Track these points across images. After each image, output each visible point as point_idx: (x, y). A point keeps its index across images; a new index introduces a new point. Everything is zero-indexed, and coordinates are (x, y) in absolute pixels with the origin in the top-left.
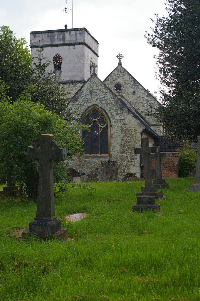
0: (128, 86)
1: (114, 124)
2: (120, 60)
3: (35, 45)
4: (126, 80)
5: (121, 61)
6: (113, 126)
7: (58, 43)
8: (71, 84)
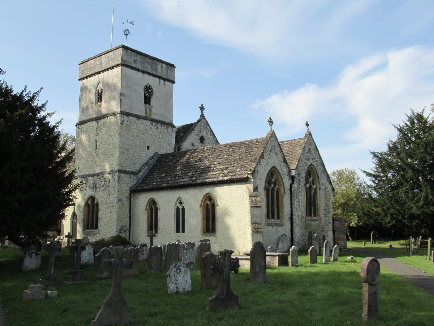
0: (209, 141)
1: (321, 187)
2: (202, 112)
3: (127, 63)
4: (207, 135)
5: (204, 113)
6: (321, 189)
7: (151, 72)
8: (163, 125)
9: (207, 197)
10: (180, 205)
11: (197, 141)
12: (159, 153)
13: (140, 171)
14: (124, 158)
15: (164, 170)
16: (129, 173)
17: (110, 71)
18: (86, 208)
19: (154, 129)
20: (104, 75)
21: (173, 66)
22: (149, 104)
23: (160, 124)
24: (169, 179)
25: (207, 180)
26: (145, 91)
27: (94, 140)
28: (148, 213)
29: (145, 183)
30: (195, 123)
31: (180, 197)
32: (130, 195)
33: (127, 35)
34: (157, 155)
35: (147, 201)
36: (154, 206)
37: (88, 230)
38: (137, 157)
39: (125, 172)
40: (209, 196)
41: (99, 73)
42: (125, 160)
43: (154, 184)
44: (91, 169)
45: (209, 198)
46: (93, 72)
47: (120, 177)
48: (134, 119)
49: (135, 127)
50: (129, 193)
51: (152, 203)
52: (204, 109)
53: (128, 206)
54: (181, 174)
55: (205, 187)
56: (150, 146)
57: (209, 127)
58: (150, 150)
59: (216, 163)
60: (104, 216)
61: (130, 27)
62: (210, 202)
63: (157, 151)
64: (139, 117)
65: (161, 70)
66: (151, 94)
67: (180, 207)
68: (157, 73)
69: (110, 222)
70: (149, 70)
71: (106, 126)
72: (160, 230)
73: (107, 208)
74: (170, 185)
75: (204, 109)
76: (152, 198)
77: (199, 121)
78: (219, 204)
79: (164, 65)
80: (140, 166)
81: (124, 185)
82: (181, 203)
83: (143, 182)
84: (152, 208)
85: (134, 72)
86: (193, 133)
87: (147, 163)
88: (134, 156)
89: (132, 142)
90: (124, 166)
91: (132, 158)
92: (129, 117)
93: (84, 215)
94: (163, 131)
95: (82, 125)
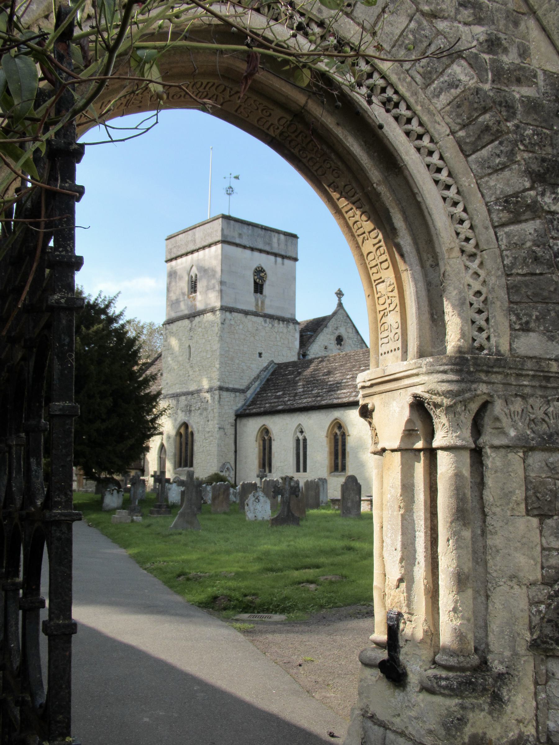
0: (350, 342)
5: (342, 302)
8: (281, 322)
9: (335, 424)
10: (300, 434)
11: (332, 342)
12: (276, 361)
13: (248, 388)
14: (226, 370)
15: (281, 385)
16: (234, 390)
17: (207, 250)
18: (178, 438)
19: (268, 329)
20: (198, 255)
21: (295, 236)
22: (261, 293)
23: (276, 321)
24: (286, 399)
25: (335, 401)
26: (255, 275)
27: (187, 345)
28: (260, 446)
29: (255, 404)
30: (329, 316)
31: (300, 424)
32: (236, 420)
33: (229, 194)
34: (273, 364)
35: (258, 429)
36: (267, 435)
37: (180, 469)
38: (245, 368)
39: (228, 390)
40: (338, 422)
41: (192, 252)
42: (227, 374)
43: (267, 405)
44: (184, 385)
45: (338, 425)
46: (183, 251)
47: (222, 397)
48: (240, 316)
49: (241, 327)
50: (234, 418)
51: (264, 432)
52: (343, 295)
53: (233, 437)
54: (303, 391)
55: (332, 410)
56: (263, 352)
57: (350, 321)
58: (263, 358)
59: (348, 377)
60: (201, 450)
61: (234, 183)
62: (340, 431)
63: (273, 359)
64: (246, 313)
65: (277, 244)
66: (263, 279)
67: (301, 437)
68: (272, 249)
69: (209, 457)
70: (261, 246)
71: (203, 327)
72: (275, 469)
73: (205, 438)
74: (287, 407)
75: (343, 295)
76: (264, 425)
77: (335, 314)
78: (350, 433)
79: (282, 237)
80: (249, 381)
81: (226, 407)
82: (302, 432)
83: (253, 402)
84: (264, 438)
85: (239, 250)
86: (326, 330)
87: (258, 376)
88: (241, 367)
89: (237, 348)
90: (227, 381)
91: (237, 371)
92: (233, 313)
93: (175, 448)
94: (281, 330)
95: (171, 325)
